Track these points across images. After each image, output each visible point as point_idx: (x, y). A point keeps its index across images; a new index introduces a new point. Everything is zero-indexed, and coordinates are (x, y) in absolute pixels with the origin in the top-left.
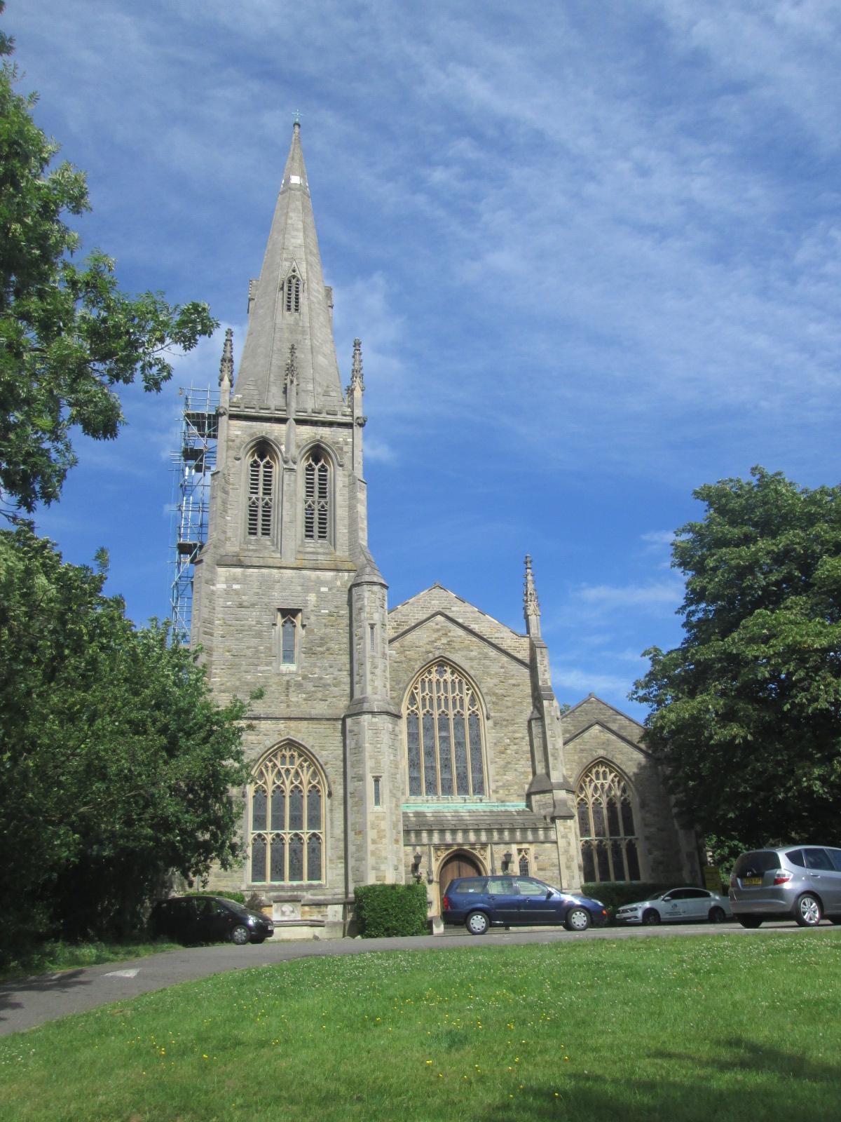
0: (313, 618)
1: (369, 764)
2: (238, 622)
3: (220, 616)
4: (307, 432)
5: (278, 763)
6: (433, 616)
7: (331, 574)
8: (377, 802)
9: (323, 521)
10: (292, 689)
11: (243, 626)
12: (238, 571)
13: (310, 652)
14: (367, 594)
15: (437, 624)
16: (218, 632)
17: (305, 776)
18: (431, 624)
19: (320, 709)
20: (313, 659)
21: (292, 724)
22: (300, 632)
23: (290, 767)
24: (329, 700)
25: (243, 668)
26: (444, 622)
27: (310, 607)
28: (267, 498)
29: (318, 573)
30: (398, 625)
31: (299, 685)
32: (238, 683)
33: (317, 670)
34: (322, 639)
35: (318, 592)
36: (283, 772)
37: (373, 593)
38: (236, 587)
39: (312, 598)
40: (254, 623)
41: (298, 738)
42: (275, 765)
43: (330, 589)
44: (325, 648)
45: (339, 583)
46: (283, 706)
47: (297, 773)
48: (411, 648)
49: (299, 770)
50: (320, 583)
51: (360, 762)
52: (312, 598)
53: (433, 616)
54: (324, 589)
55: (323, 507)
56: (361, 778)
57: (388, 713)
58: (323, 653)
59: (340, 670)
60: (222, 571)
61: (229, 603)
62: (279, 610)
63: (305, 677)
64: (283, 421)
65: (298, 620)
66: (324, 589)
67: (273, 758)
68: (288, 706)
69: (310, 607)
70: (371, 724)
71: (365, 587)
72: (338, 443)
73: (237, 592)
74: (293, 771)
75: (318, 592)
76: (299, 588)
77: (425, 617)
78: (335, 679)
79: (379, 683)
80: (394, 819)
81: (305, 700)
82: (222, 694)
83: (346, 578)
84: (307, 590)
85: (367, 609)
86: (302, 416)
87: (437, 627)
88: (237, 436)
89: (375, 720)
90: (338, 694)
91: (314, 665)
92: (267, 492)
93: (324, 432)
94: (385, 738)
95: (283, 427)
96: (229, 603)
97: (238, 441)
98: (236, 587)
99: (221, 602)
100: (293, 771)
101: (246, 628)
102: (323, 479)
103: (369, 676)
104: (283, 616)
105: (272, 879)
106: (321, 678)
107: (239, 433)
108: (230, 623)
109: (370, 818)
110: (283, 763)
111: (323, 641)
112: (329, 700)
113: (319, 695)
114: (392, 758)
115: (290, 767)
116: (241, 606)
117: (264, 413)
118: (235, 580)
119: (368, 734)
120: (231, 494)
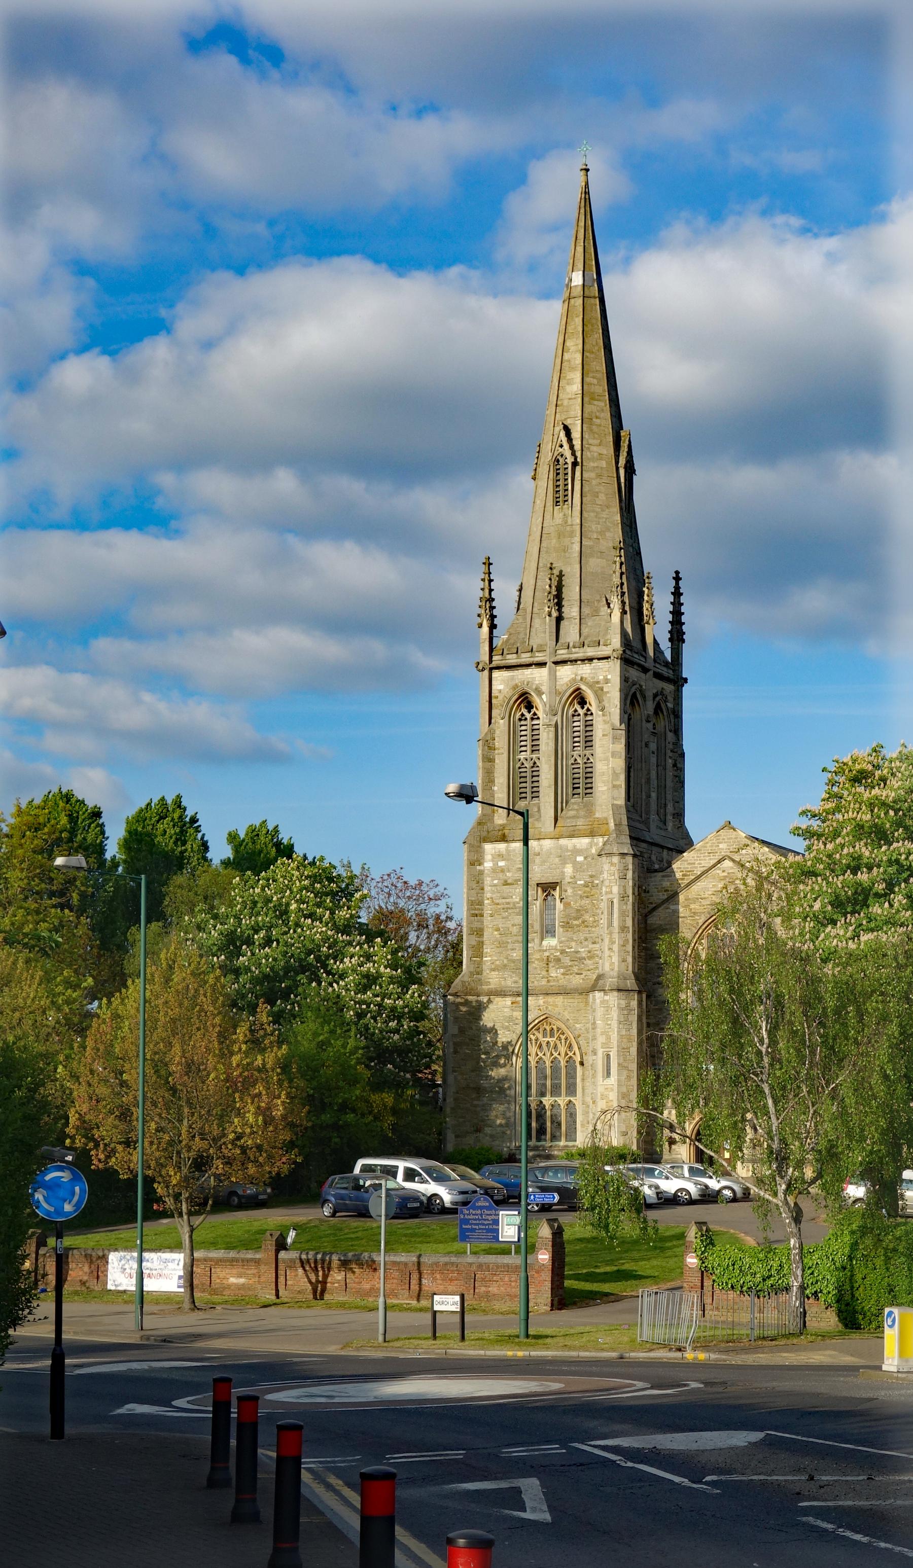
0: (570, 891)
1: (601, 1039)
2: (504, 900)
3: (489, 895)
4: (566, 673)
5: (540, 1036)
6: (719, 862)
7: (585, 841)
8: (608, 1074)
9: (589, 775)
10: (551, 965)
11: (508, 903)
12: (502, 846)
13: (567, 925)
14: (606, 867)
15: (724, 871)
16: (487, 912)
17: (562, 1049)
18: (717, 872)
19: (576, 981)
20: (569, 934)
21: (550, 999)
22: (559, 906)
23: (550, 1040)
24: (584, 973)
25: (510, 946)
26: (732, 868)
27: (568, 880)
28: (534, 756)
29: (575, 841)
30: (683, 875)
31: (558, 960)
32: (505, 961)
33: (573, 944)
34: (578, 911)
35: (575, 863)
36: (544, 1045)
37: (612, 864)
38: (501, 864)
39: (569, 870)
40: (517, 900)
41: (551, 1010)
42: (537, 1040)
43: (585, 858)
44: (580, 921)
45: (593, 851)
46: (544, 982)
47: (555, 1047)
48: (695, 900)
49: (558, 1042)
50: (576, 851)
51: (594, 1038)
52: (569, 870)
53: (719, 862)
54: (580, 859)
55: (588, 759)
56: (595, 1053)
57: (619, 990)
58: (578, 926)
59: (594, 943)
60: (488, 847)
61: (496, 882)
62: (538, 885)
63: (563, 952)
64: (542, 664)
65: (557, 894)
66: (580, 859)
67: (536, 1033)
68: (548, 981)
69: (568, 880)
70: (603, 1002)
71: (604, 858)
72: (598, 682)
73: (502, 871)
74: (552, 1044)
75: (575, 863)
76: (557, 860)
77: (713, 862)
78: (589, 952)
79: (615, 959)
80: (624, 1090)
81: (563, 974)
82: (493, 973)
83: (601, 844)
84: (564, 861)
85: (607, 883)
86: (563, 654)
87: (725, 874)
88: (500, 691)
89: (607, 998)
90: (592, 967)
91: (572, 940)
92: (535, 749)
93: (585, 670)
94: (614, 1014)
95: (544, 671)
96: (496, 882)
97: (501, 697)
98: (501, 864)
99: (488, 881)
100: (552, 1044)
101: (511, 906)
102: (589, 725)
103: (607, 953)
104: (544, 891)
105: (538, 1139)
106: (577, 952)
107: (501, 687)
108: (497, 901)
109: (600, 1089)
110: (544, 1036)
111: (579, 912)
112: (584, 973)
113: (575, 969)
114: (624, 1033)
115: (550, 1040)
116: (506, 883)
117: (525, 658)
118: (500, 856)
119: (600, 1012)
120: (497, 761)
